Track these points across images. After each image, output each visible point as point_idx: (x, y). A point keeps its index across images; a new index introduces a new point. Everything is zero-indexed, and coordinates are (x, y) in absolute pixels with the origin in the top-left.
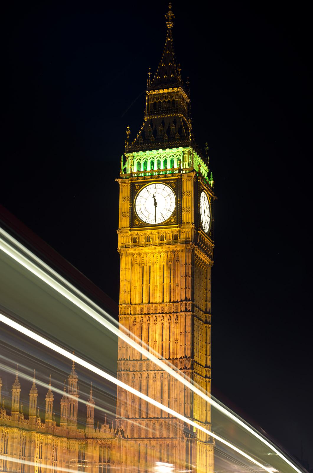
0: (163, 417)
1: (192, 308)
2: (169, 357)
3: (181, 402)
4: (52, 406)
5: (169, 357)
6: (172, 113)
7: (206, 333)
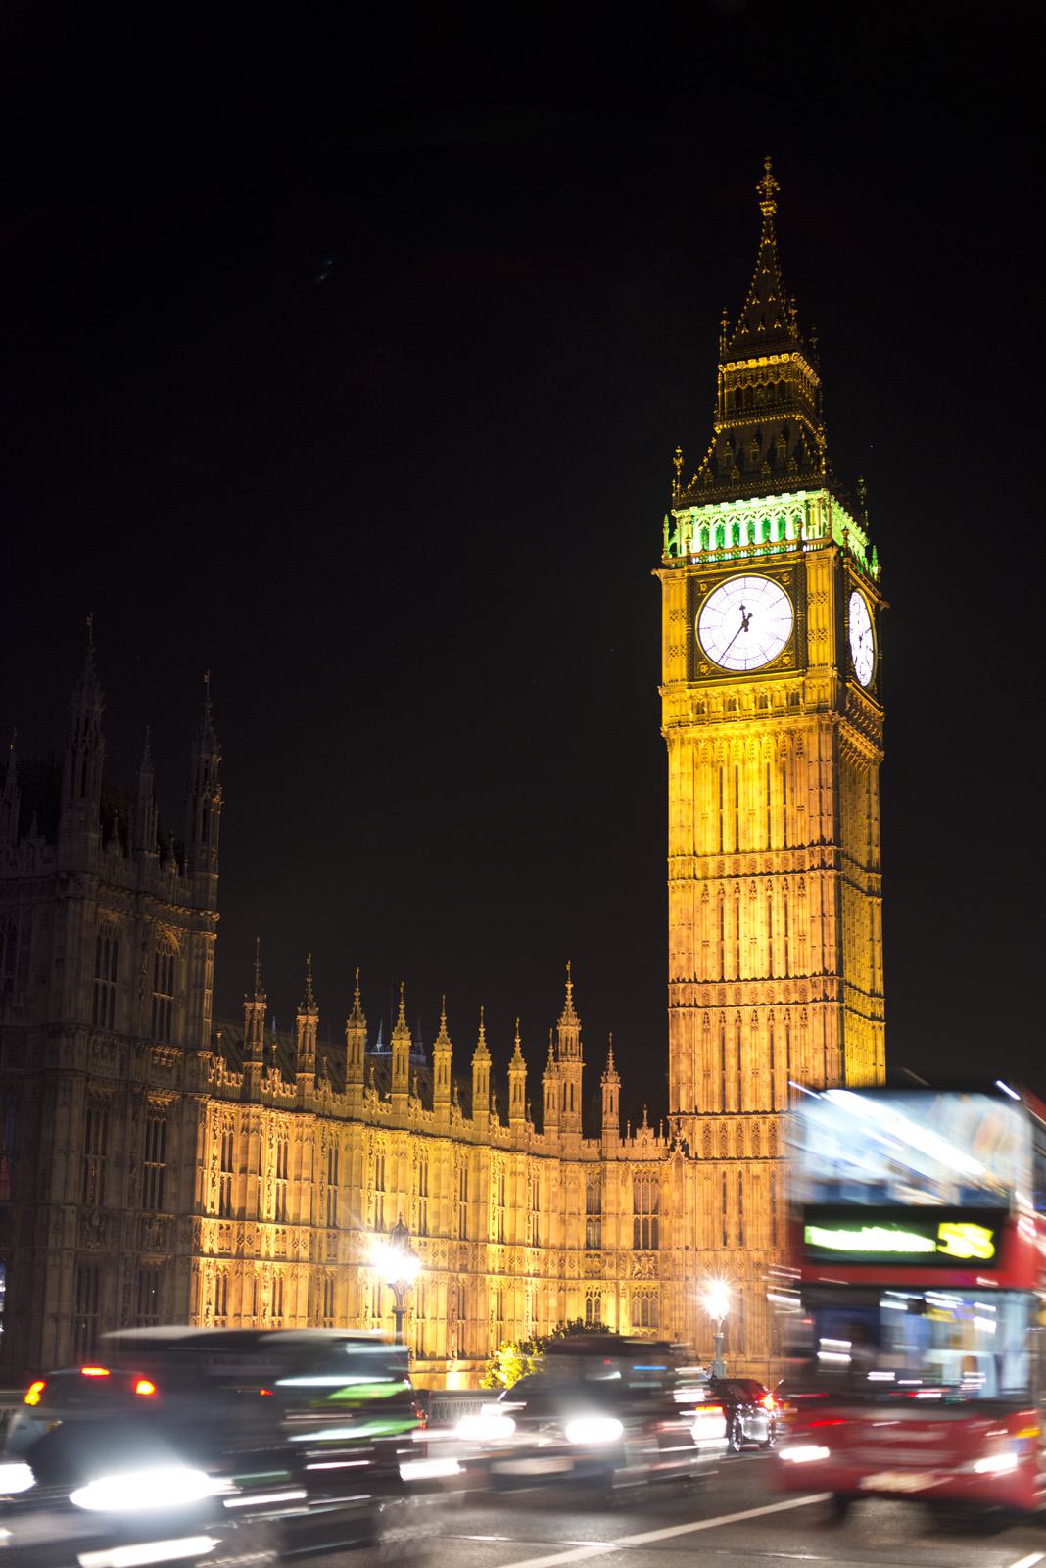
1: (838, 860)
2: (787, 974)
4: (523, 1088)
5: (787, 974)
6: (779, 412)
7: (872, 915)
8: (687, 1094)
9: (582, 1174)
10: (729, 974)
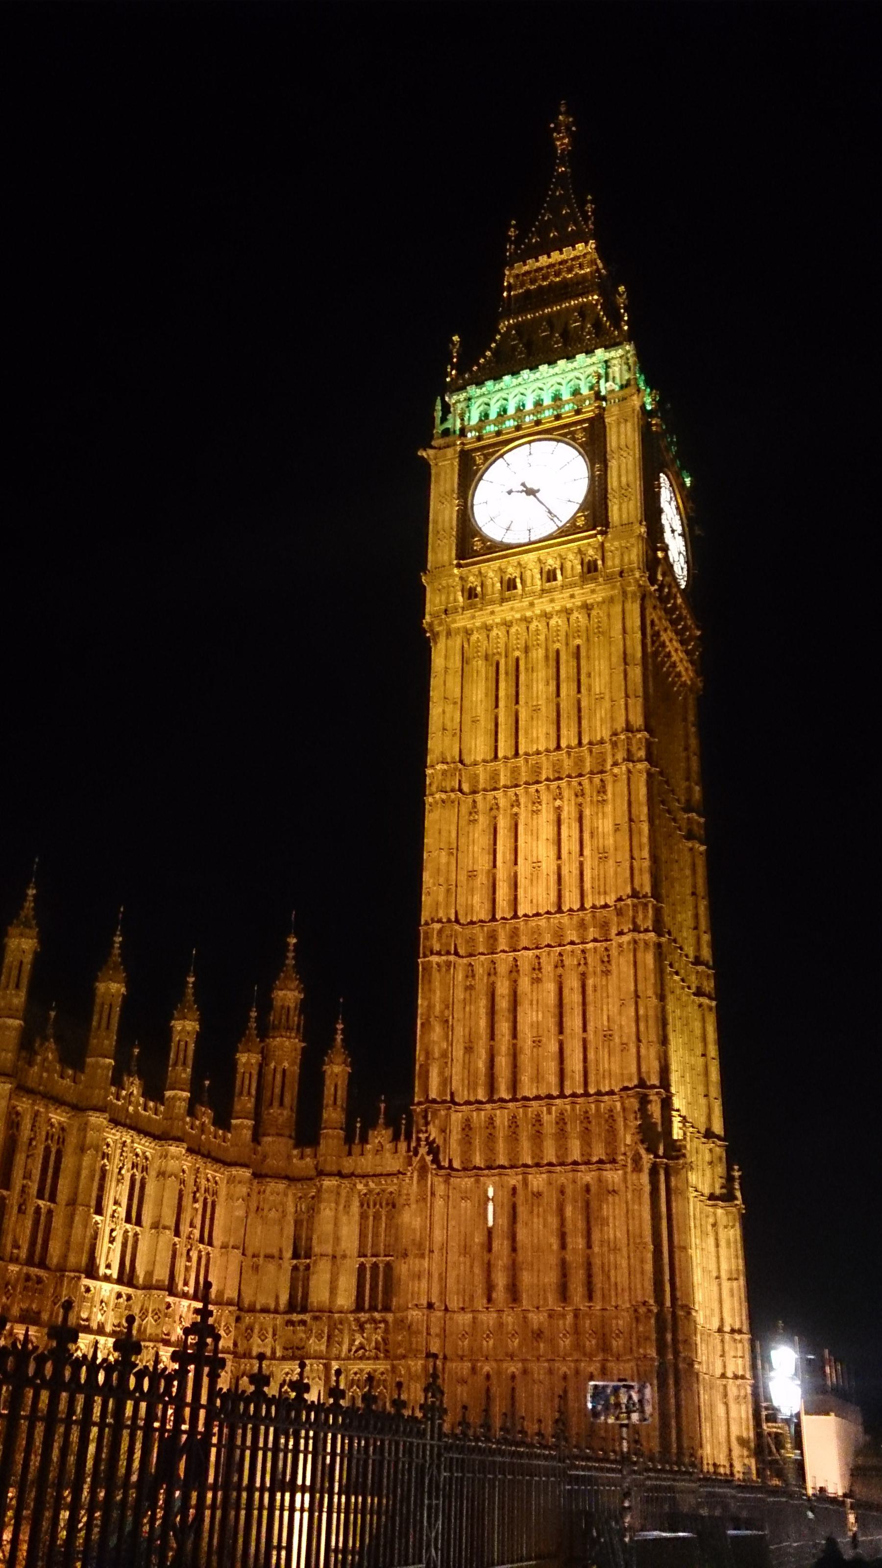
0: (568, 1092)
3: (625, 1040)
4: (192, 1046)
8: (441, 1073)
9: (290, 1197)
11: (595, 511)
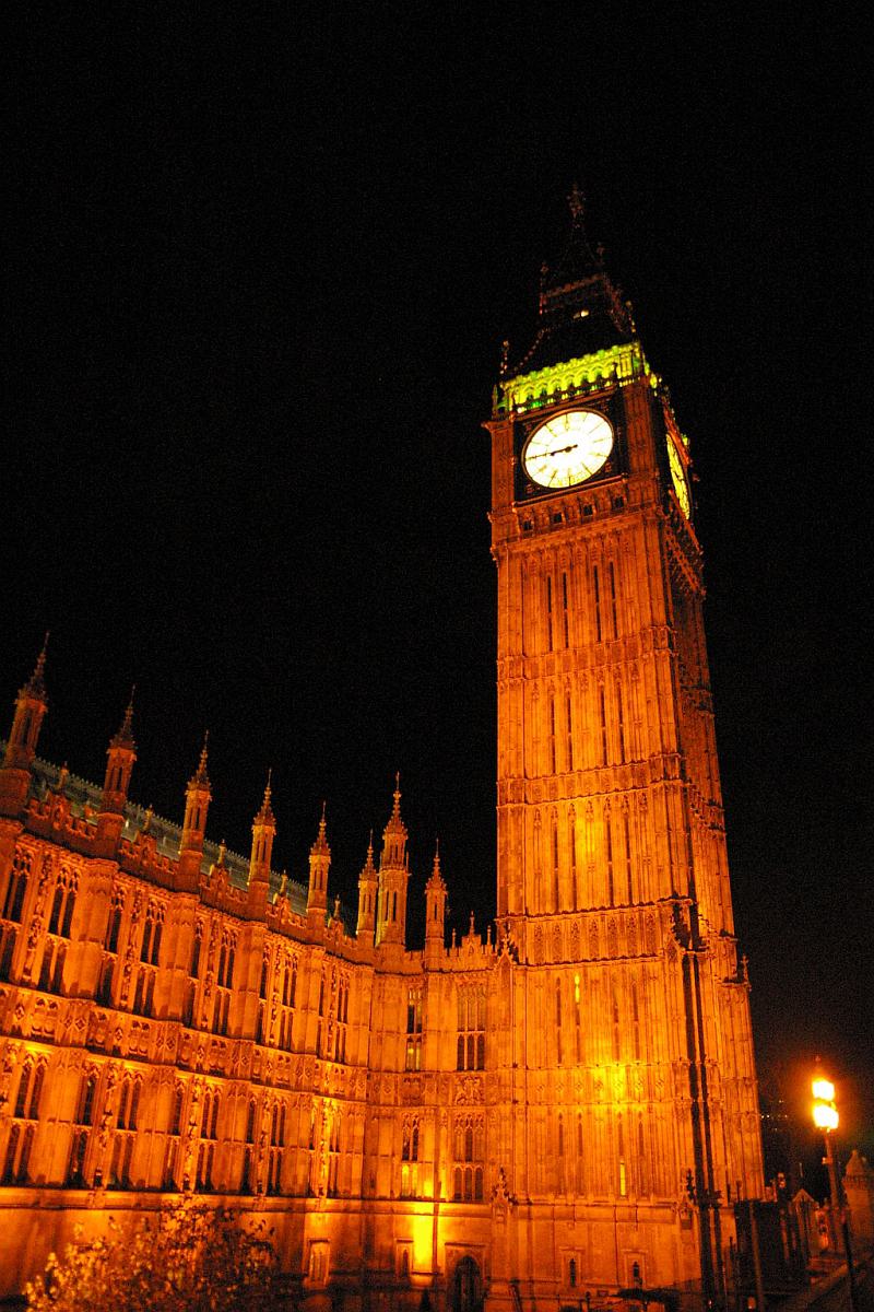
8: (517, 892)
10: (561, 766)
11: (619, 461)
